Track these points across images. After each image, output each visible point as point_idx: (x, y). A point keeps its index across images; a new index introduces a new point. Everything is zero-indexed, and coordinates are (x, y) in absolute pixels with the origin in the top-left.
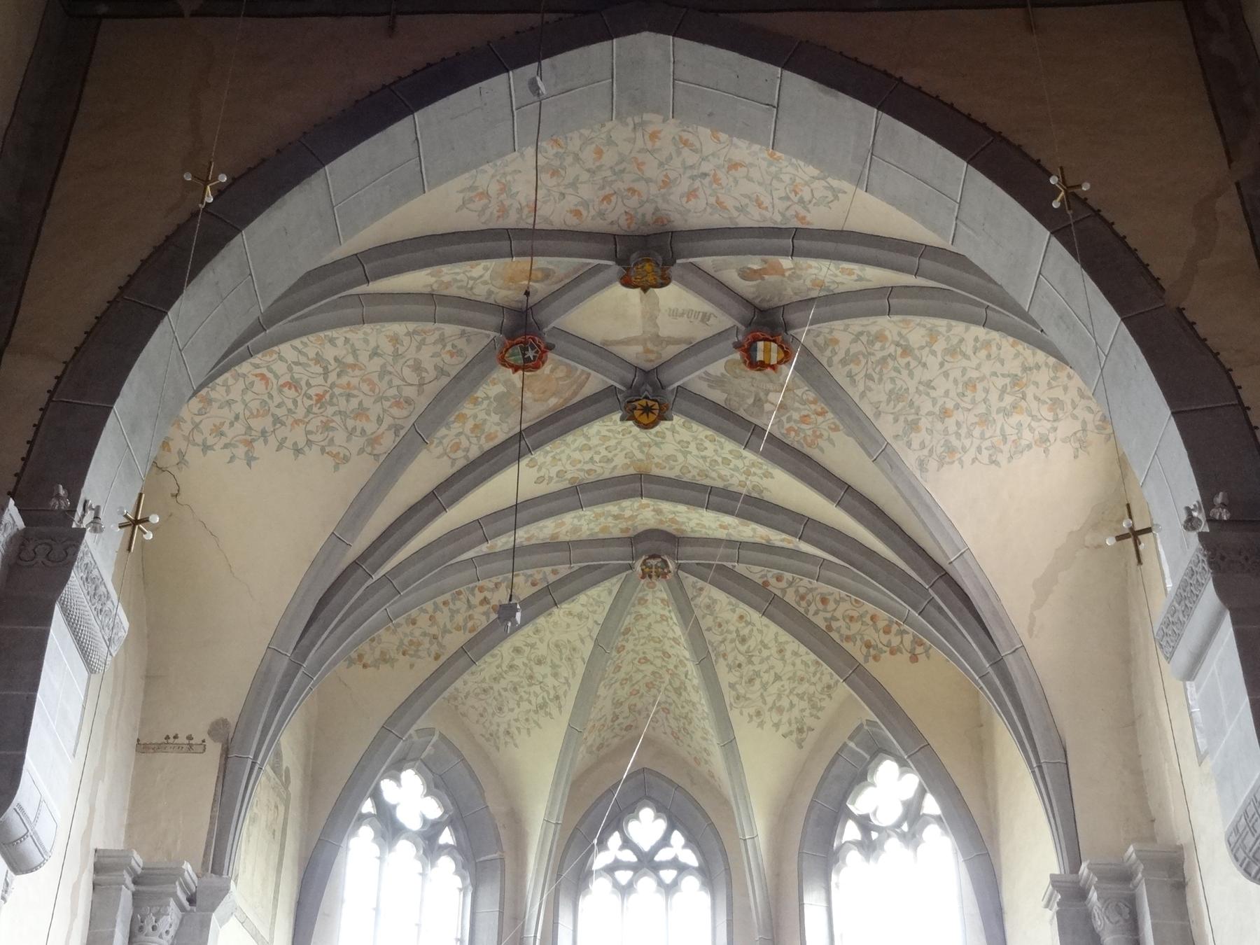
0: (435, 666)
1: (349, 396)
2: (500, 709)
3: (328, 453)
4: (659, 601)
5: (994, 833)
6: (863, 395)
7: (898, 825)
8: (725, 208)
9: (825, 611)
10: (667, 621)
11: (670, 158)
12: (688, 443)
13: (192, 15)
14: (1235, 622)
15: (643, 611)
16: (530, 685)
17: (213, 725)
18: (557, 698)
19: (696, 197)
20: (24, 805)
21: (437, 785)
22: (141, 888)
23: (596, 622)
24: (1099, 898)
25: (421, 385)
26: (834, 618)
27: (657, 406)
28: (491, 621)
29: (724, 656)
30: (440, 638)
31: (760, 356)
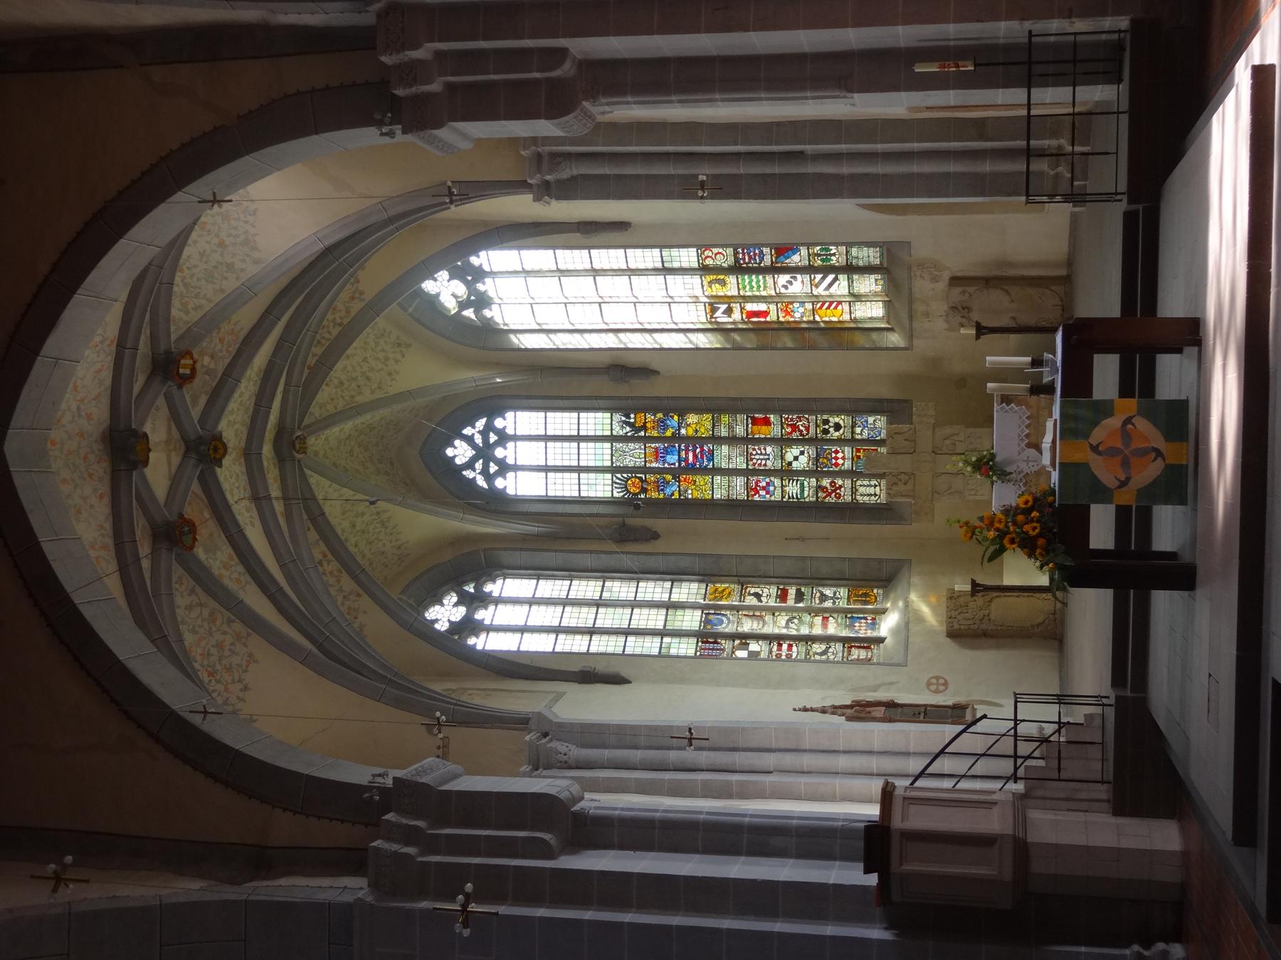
0: (365, 597)
1: (209, 654)
2: (383, 553)
3: (247, 668)
4: (317, 442)
5: (485, 223)
6: (209, 301)
7: (467, 284)
8: (99, 394)
9: (328, 327)
10: (328, 437)
11: (66, 431)
12: (229, 421)
14: (456, 120)
15: (322, 453)
16: (368, 532)
18: (378, 513)
19: (91, 414)
20: (556, 791)
22: (541, 765)
23: (330, 486)
24: (550, 175)
25: (201, 605)
26: (334, 321)
27: (213, 442)
28: (333, 559)
29: (352, 397)
30: (345, 594)
31: (188, 371)
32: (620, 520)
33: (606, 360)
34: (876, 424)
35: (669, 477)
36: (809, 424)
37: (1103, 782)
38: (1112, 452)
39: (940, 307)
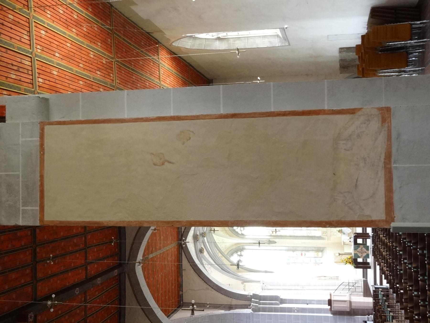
2: (223, 247)
13: (183, 292)
17: (242, 284)
21: (232, 255)
32: (269, 239)
37: (362, 292)
38: (360, 252)
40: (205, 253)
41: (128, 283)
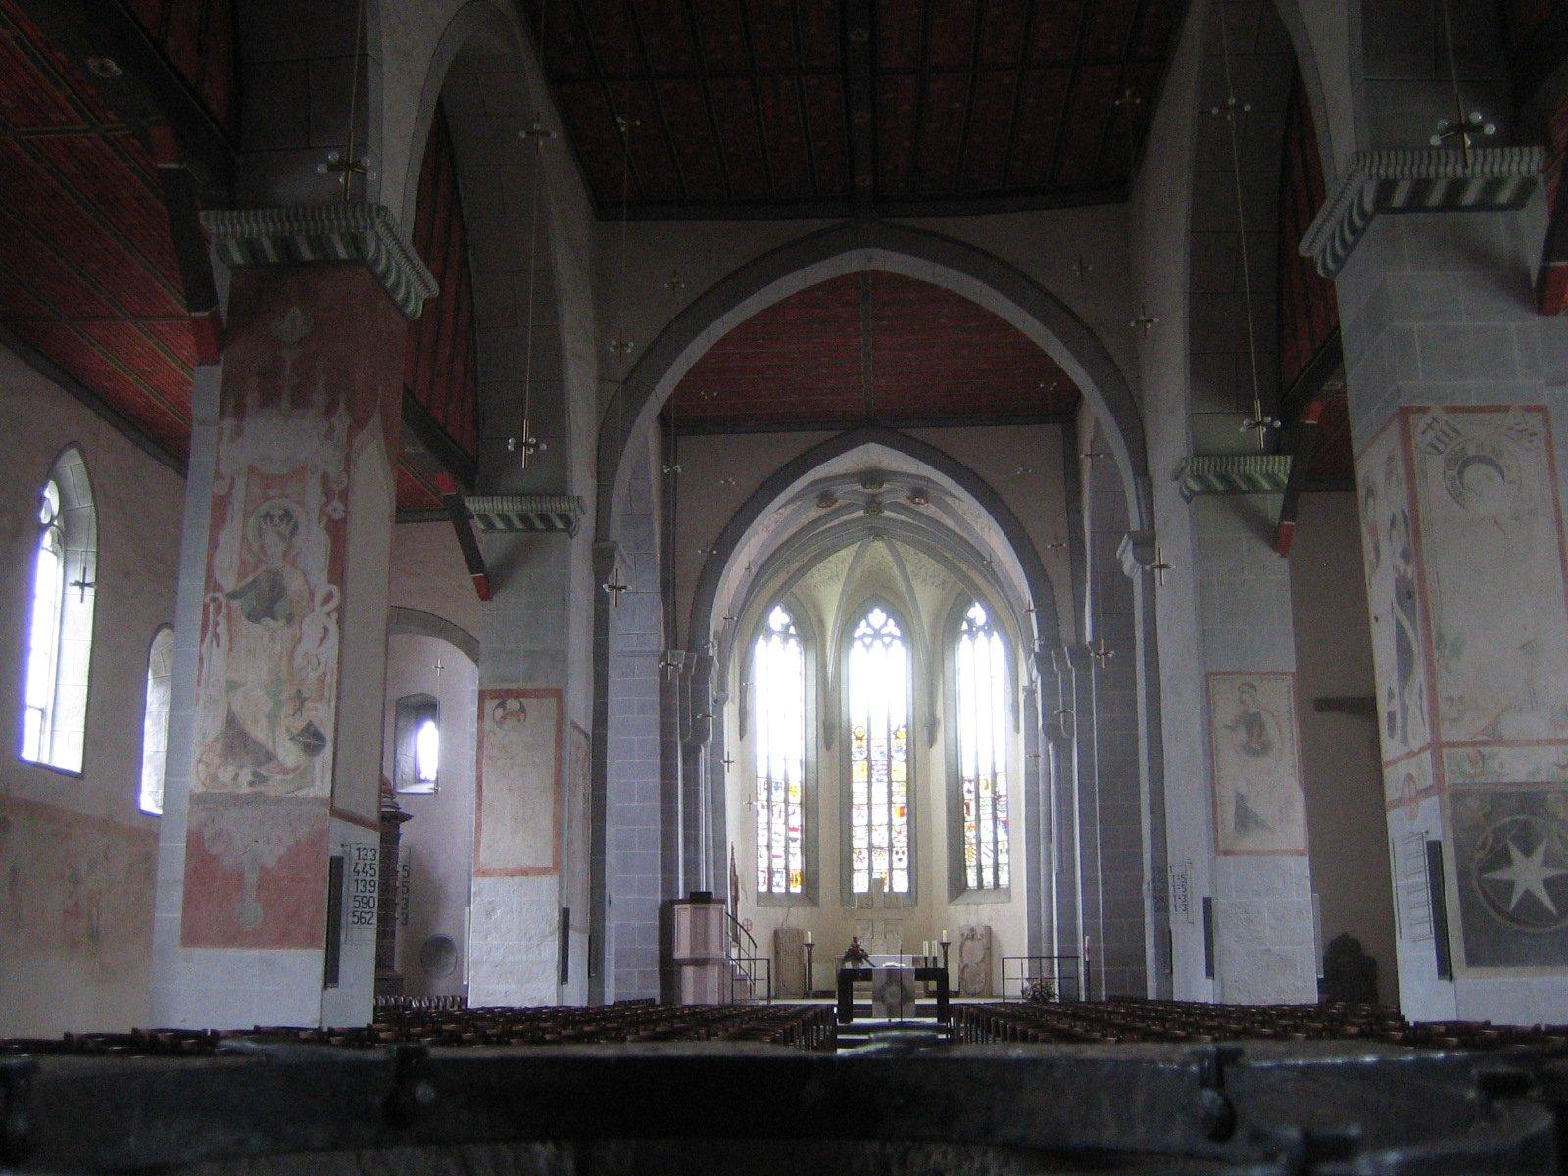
33: (939, 714)
34: (901, 884)
35: (865, 754)
36: (901, 842)
39: (973, 921)
40: (815, 513)
41: (817, 224)
